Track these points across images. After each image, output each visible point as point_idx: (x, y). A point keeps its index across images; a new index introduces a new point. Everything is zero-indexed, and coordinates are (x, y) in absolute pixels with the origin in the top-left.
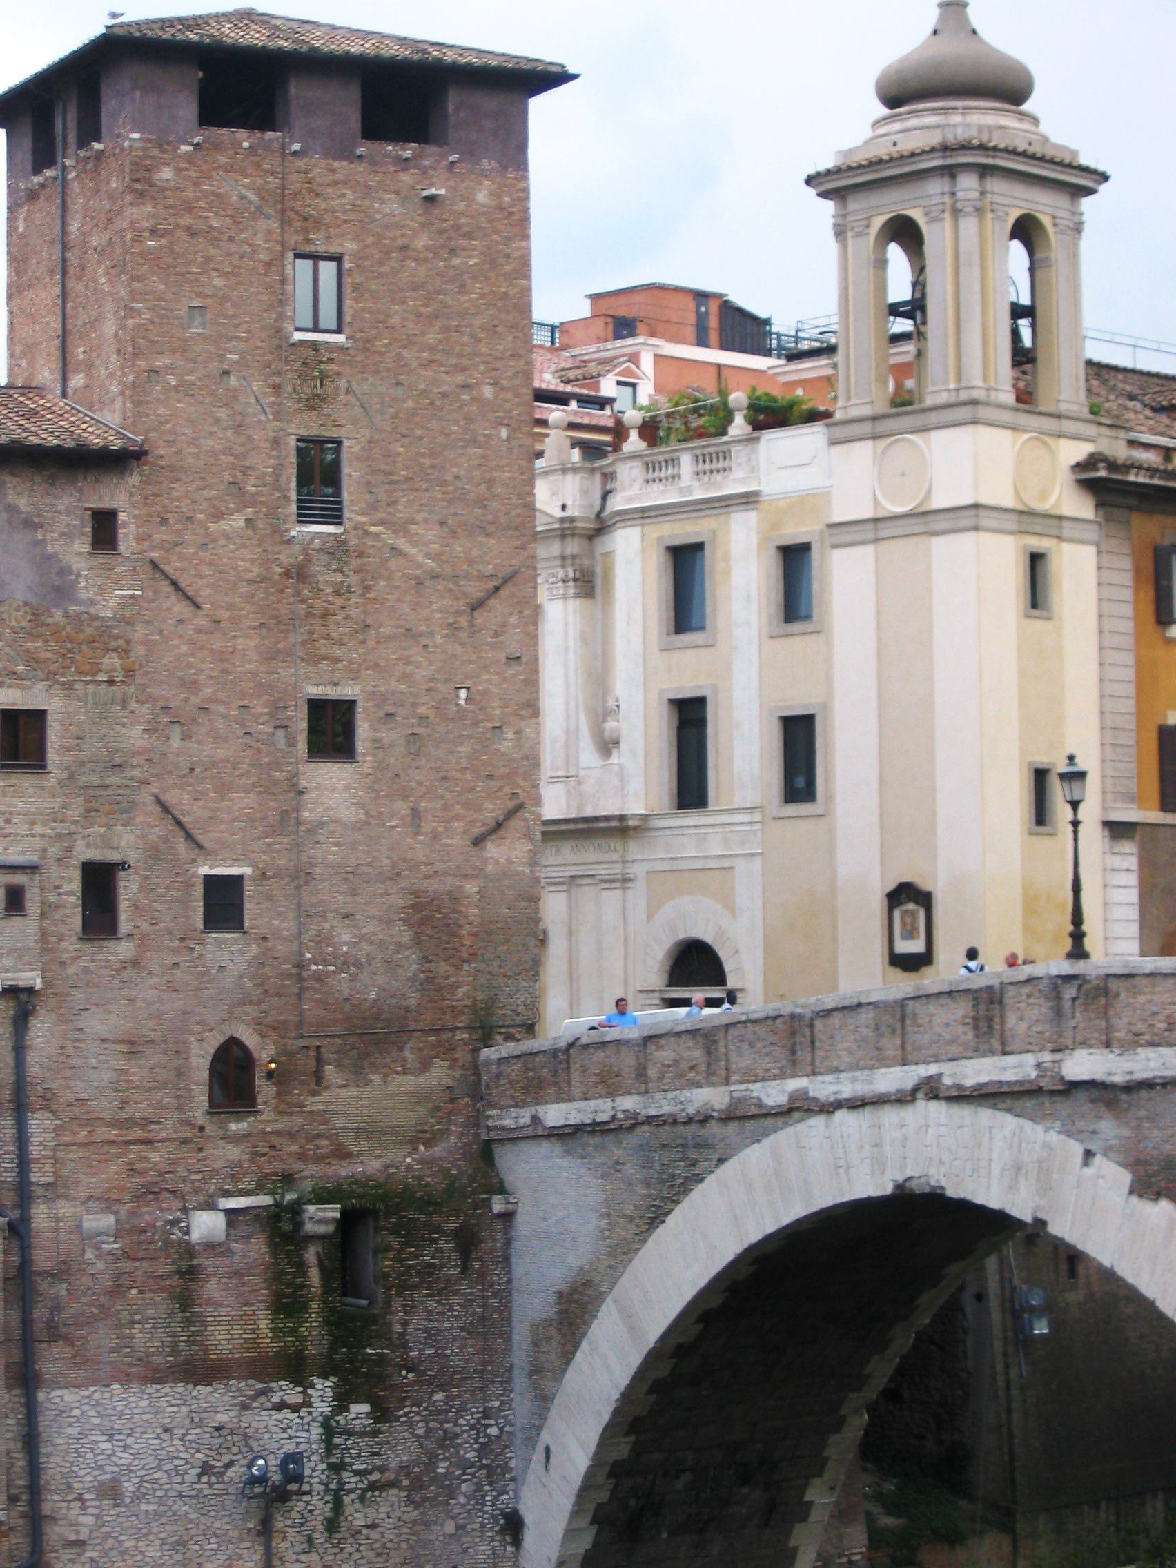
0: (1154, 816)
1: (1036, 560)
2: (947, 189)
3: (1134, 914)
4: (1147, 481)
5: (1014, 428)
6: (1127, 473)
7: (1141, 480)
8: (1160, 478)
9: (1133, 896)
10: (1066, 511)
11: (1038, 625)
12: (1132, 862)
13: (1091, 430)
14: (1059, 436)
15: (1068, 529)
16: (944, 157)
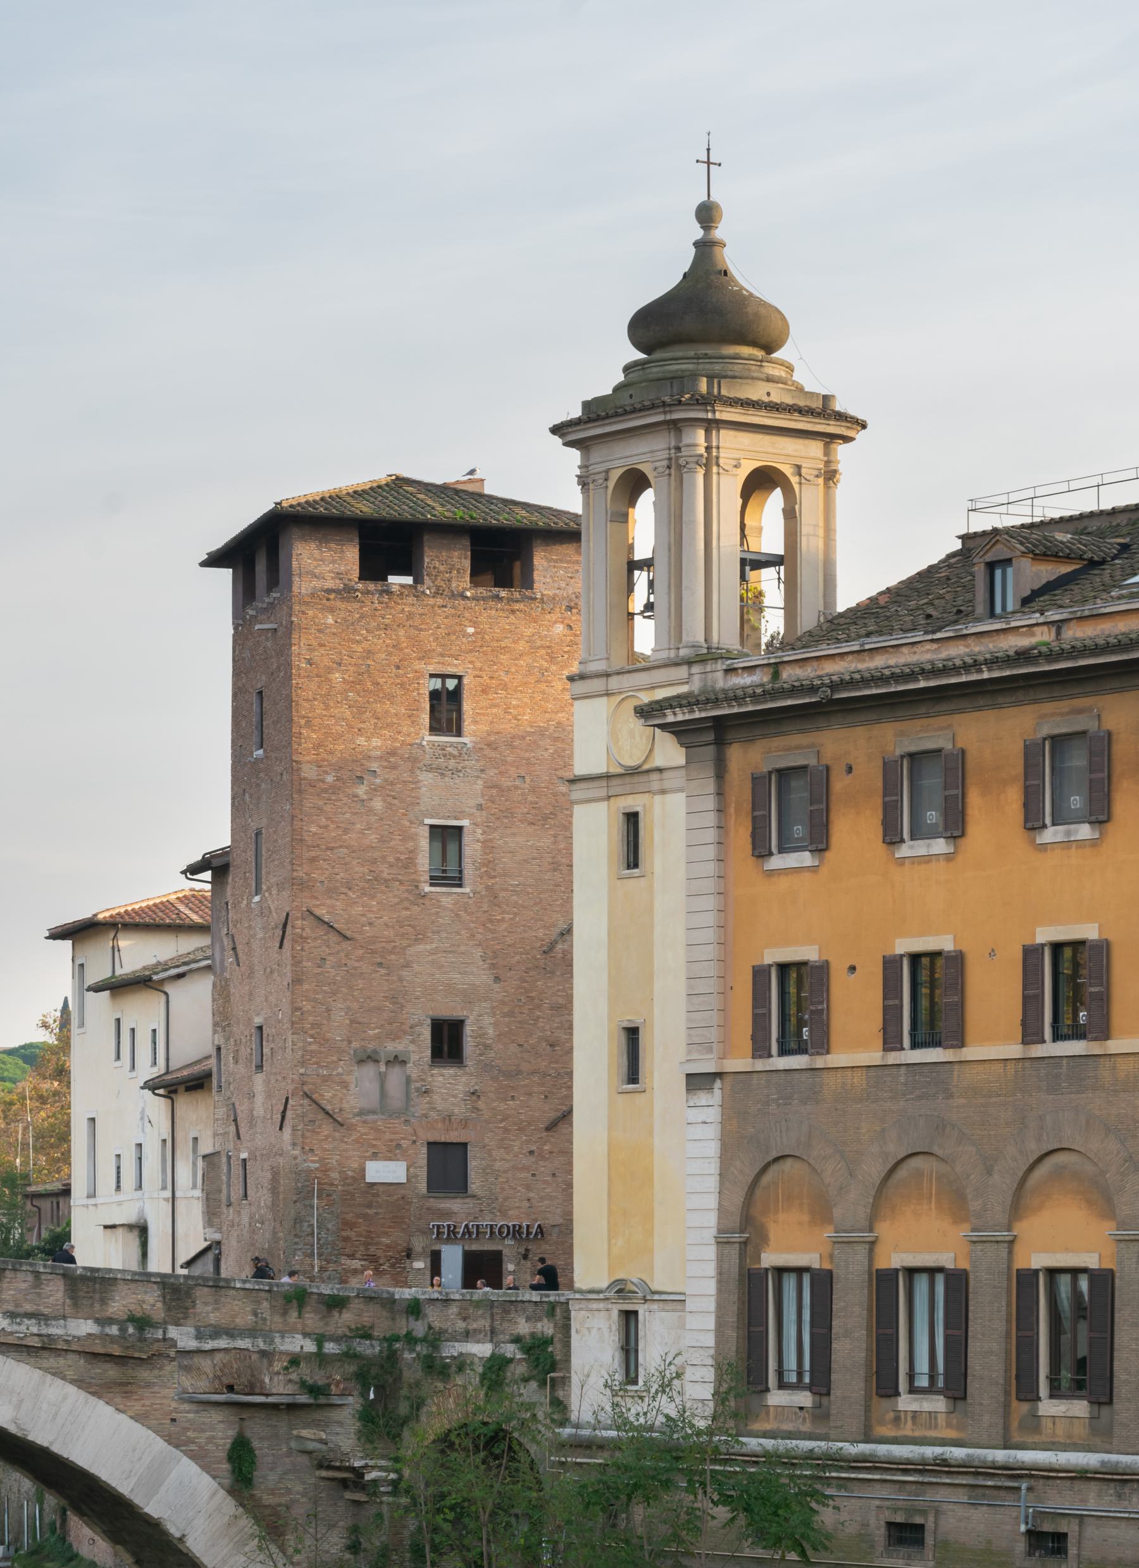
0: (740, 1063)
1: (632, 819)
2: (673, 444)
3: (713, 1168)
4: (688, 717)
5: (608, 694)
6: (665, 715)
7: (680, 718)
8: (700, 710)
9: (712, 1149)
10: (658, 761)
11: (633, 885)
12: (713, 1114)
13: (682, 672)
14: (653, 688)
15: (655, 781)
16: (665, 413)
